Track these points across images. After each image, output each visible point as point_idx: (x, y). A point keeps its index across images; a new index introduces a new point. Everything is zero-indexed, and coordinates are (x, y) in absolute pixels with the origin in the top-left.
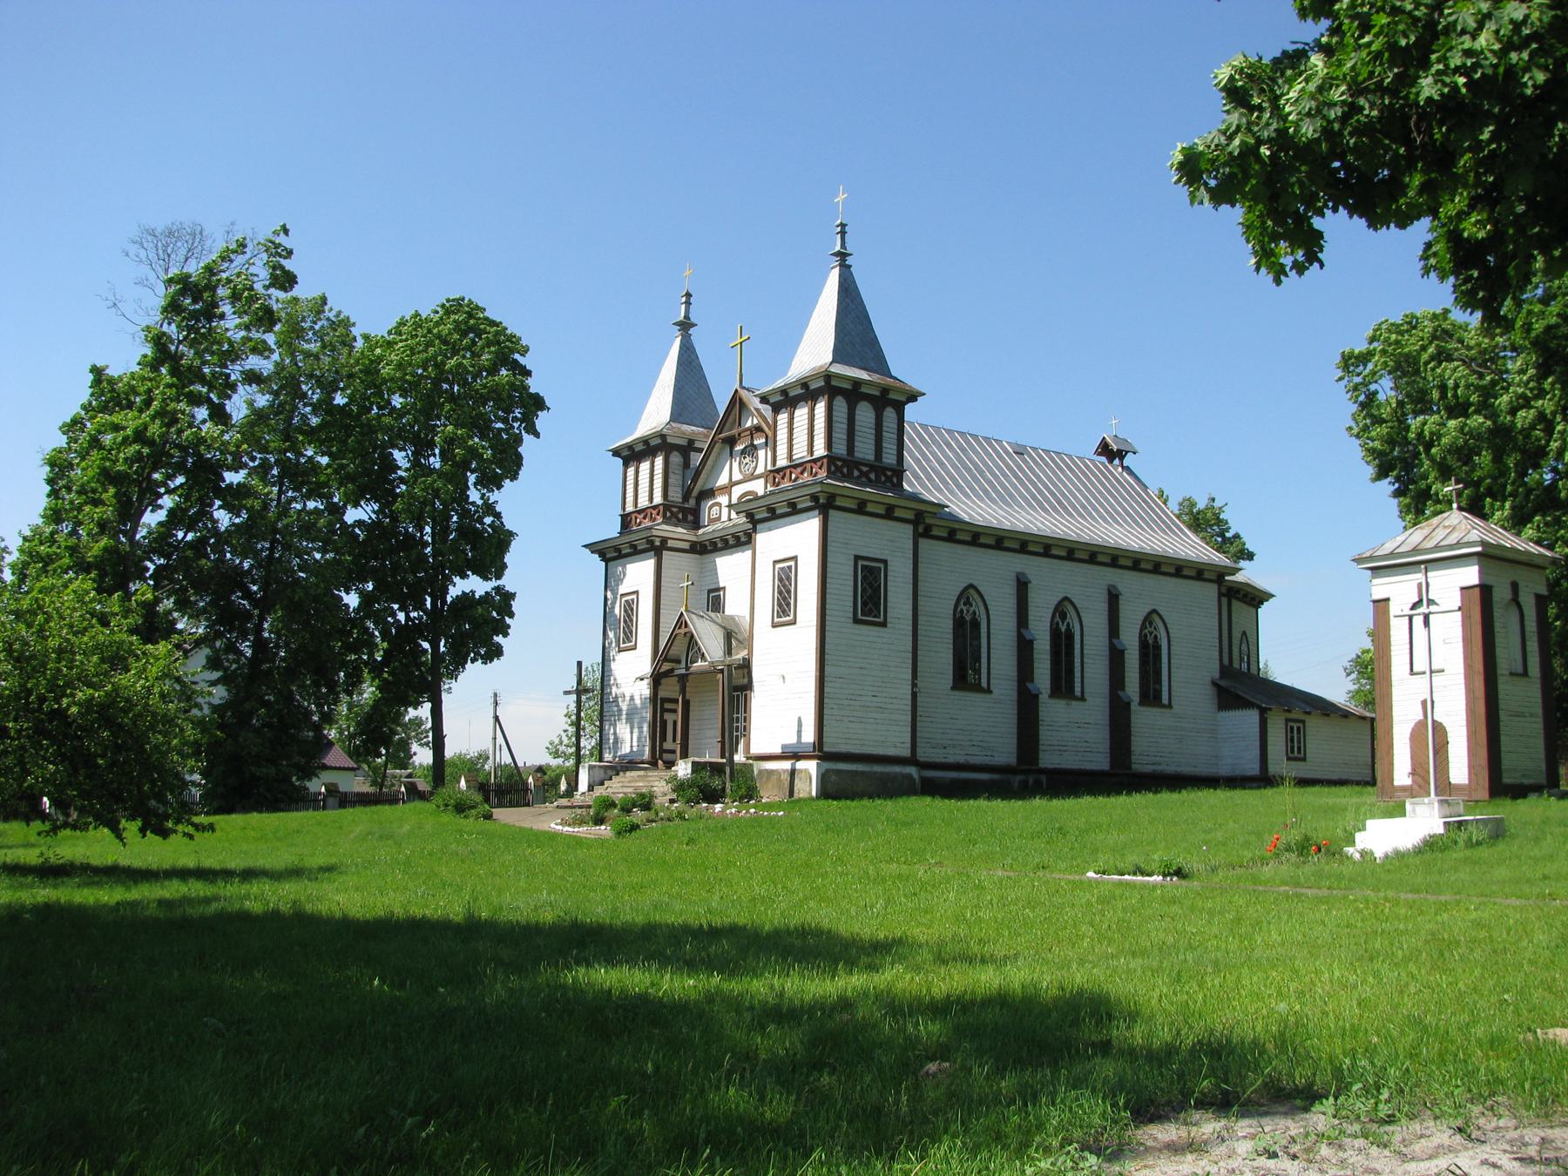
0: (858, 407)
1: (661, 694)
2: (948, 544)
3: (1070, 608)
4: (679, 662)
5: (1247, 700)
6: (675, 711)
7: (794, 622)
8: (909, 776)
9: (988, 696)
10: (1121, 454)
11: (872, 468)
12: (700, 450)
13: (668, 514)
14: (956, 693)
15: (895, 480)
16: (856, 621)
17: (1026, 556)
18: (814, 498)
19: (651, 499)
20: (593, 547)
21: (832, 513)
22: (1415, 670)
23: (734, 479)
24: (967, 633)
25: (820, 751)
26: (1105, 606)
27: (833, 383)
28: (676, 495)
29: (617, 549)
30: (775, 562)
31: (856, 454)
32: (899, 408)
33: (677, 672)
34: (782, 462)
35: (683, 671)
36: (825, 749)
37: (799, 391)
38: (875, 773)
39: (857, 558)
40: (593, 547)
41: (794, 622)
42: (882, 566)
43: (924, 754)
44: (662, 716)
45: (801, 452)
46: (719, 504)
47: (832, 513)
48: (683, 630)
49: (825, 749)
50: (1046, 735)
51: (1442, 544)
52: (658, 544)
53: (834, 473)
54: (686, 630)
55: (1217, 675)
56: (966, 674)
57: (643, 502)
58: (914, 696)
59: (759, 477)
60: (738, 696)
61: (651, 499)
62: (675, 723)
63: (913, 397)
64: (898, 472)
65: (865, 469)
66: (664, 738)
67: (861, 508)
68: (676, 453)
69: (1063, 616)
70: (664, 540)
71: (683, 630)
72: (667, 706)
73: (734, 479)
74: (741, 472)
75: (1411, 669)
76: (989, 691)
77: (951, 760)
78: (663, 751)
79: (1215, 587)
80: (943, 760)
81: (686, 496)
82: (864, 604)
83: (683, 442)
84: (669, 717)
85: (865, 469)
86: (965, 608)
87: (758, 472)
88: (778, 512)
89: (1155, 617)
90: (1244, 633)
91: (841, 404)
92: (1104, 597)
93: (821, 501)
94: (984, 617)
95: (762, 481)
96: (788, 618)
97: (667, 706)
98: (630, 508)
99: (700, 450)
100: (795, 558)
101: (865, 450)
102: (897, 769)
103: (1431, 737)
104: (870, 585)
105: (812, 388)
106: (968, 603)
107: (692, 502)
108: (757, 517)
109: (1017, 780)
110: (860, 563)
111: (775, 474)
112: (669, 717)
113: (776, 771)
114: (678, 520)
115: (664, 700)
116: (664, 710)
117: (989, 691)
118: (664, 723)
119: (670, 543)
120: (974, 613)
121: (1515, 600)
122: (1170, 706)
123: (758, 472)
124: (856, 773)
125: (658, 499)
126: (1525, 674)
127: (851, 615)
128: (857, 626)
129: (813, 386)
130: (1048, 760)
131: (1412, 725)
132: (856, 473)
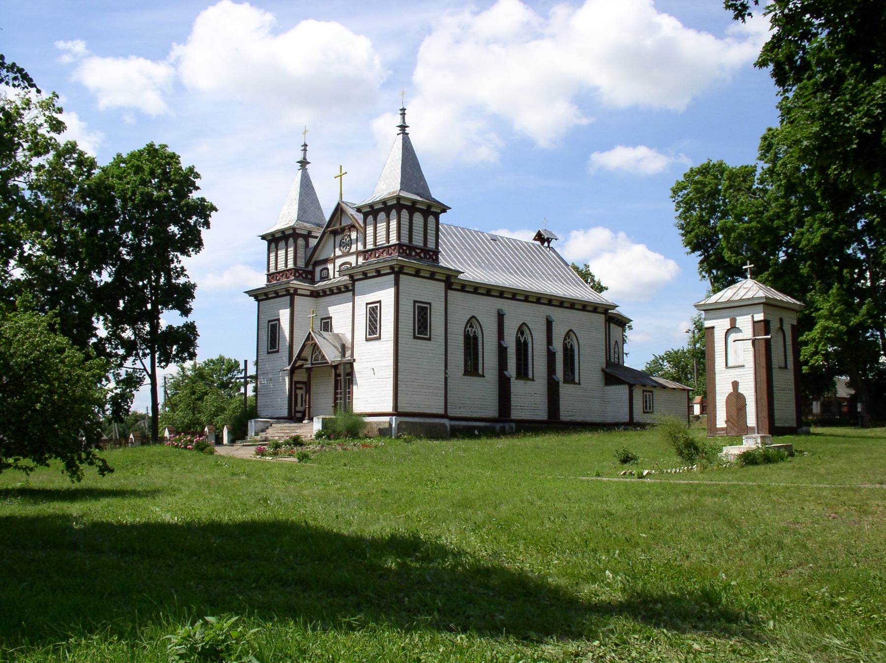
0: (415, 216)
1: (295, 379)
2: (486, 297)
3: (526, 328)
4: (306, 360)
5: (620, 379)
6: (301, 388)
7: (379, 338)
8: (444, 425)
9: (482, 378)
10: (549, 240)
11: (422, 250)
12: (316, 237)
13: (297, 274)
14: (466, 377)
15: (434, 257)
16: (415, 337)
17: (490, 298)
18: (392, 267)
19: (286, 265)
20: (250, 293)
21: (402, 277)
22: (730, 365)
23: (336, 255)
24: (471, 344)
25: (397, 413)
26: (544, 328)
27: (402, 202)
28: (301, 264)
29: (266, 294)
30: (367, 304)
31: (414, 243)
32: (436, 216)
33: (305, 366)
34: (370, 246)
35: (309, 366)
36: (399, 410)
37: (381, 206)
38: (426, 423)
39: (415, 302)
40: (250, 293)
41: (379, 338)
42: (428, 306)
43: (451, 412)
44: (295, 392)
45: (381, 241)
47: (402, 277)
48: (310, 342)
49: (399, 410)
50: (515, 401)
51: (744, 298)
53: (402, 253)
55: (604, 366)
56: (472, 368)
57: (281, 266)
58: (446, 379)
59: (353, 254)
61: (286, 265)
63: (444, 209)
64: (436, 252)
65: (418, 251)
66: (296, 405)
67: (417, 274)
68: (301, 239)
69: (522, 333)
70: (296, 290)
72: (298, 386)
73: (336, 255)
75: (726, 365)
76: (483, 376)
77: (464, 415)
78: (296, 412)
79: (603, 316)
80: (460, 415)
81: (307, 264)
82: (419, 328)
83: (305, 233)
84: (299, 392)
85: (418, 251)
86: (470, 329)
87: (351, 251)
88: (369, 275)
89: (571, 333)
90: (616, 342)
91: (405, 214)
92: (544, 322)
93: (396, 269)
94: (480, 334)
95: (355, 256)
97: (298, 386)
98: (272, 270)
99: (316, 237)
100: (380, 302)
101: (418, 241)
102: (437, 420)
103: (736, 400)
104: (422, 317)
105: (388, 204)
106: (471, 326)
107: (310, 268)
108: (356, 278)
109: (498, 426)
110: (417, 304)
111: (365, 253)
112: (299, 392)
114: (303, 278)
115: (296, 382)
116: (296, 388)
117: (483, 376)
118: (296, 395)
119: (299, 292)
120: (475, 332)
121: (781, 328)
122: (579, 384)
123: (351, 251)
124: (415, 423)
125: (291, 265)
126: (786, 367)
127: (412, 334)
128: (415, 340)
129: (389, 203)
130: (516, 414)
131: (727, 395)
132: (414, 254)
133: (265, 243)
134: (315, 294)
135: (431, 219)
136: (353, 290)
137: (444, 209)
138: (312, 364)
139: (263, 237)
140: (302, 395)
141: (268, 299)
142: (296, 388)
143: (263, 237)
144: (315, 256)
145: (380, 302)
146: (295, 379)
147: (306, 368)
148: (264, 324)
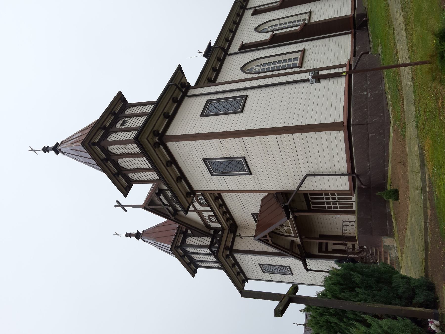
1: (316, 251)
4: (293, 242)
6: (327, 244)
28: (207, 241)
52: (228, 253)
54: (268, 236)
60: (313, 204)
62: (334, 244)
63: (120, 98)
70: (226, 248)
71: (269, 238)
84: (331, 247)
91: (113, 137)
97: (324, 248)
112: (331, 247)
115: (320, 250)
116: (327, 251)
118: (335, 251)
133: (199, 270)
135: (129, 111)
137: (120, 98)
139: (193, 272)
140: (334, 244)
142: (327, 251)
143: (193, 272)
144: (200, 228)
148: (267, 276)
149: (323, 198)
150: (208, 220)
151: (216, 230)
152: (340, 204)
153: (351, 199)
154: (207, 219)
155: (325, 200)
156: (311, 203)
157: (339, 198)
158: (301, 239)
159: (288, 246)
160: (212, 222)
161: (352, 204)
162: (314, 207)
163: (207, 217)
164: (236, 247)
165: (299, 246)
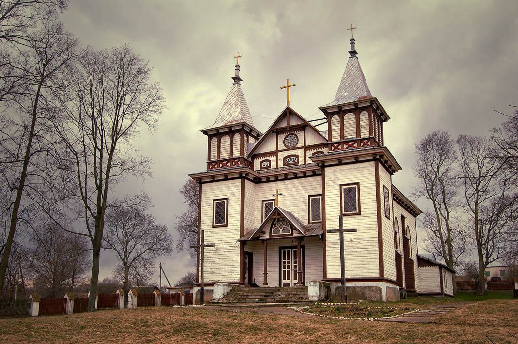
1: (245, 249)
4: (264, 233)
7: (359, 214)
19: (231, 153)
28: (245, 156)
33: (261, 238)
35: (268, 237)
45: (350, 134)
46: (269, 161)
52: (244, 175)
60: (288, 252)
74: (285, 145)
81: (248, 157)
95: (302, 151)
96: (354, 212)
98: (214, 157)
100: (358, 184)
113: (352, 287)
115: (247, 253)
133: (206, 137)
134: (257, 181)
136: (322, 175)
138: (270, 236)
139: (205, 132)
141: (214, 181)
143: (205, 132)
145: (358, 184)
146: (245, 249)
147: (262, 240)
149: (295, 258)
150: (266, 158)
151: (251, 165)
152: (289, 271)
153: (295, 278)
154: (268, 158)
155: (293, 260)
156: (290, 250)
157: (295, 271)
158: (267, 240)
159: (264, 230)
160: (262, 162)
161: (289, 279)
162: (284, 252)
163: (268, 158)
164: (247, 182)
165: (259, 237)
